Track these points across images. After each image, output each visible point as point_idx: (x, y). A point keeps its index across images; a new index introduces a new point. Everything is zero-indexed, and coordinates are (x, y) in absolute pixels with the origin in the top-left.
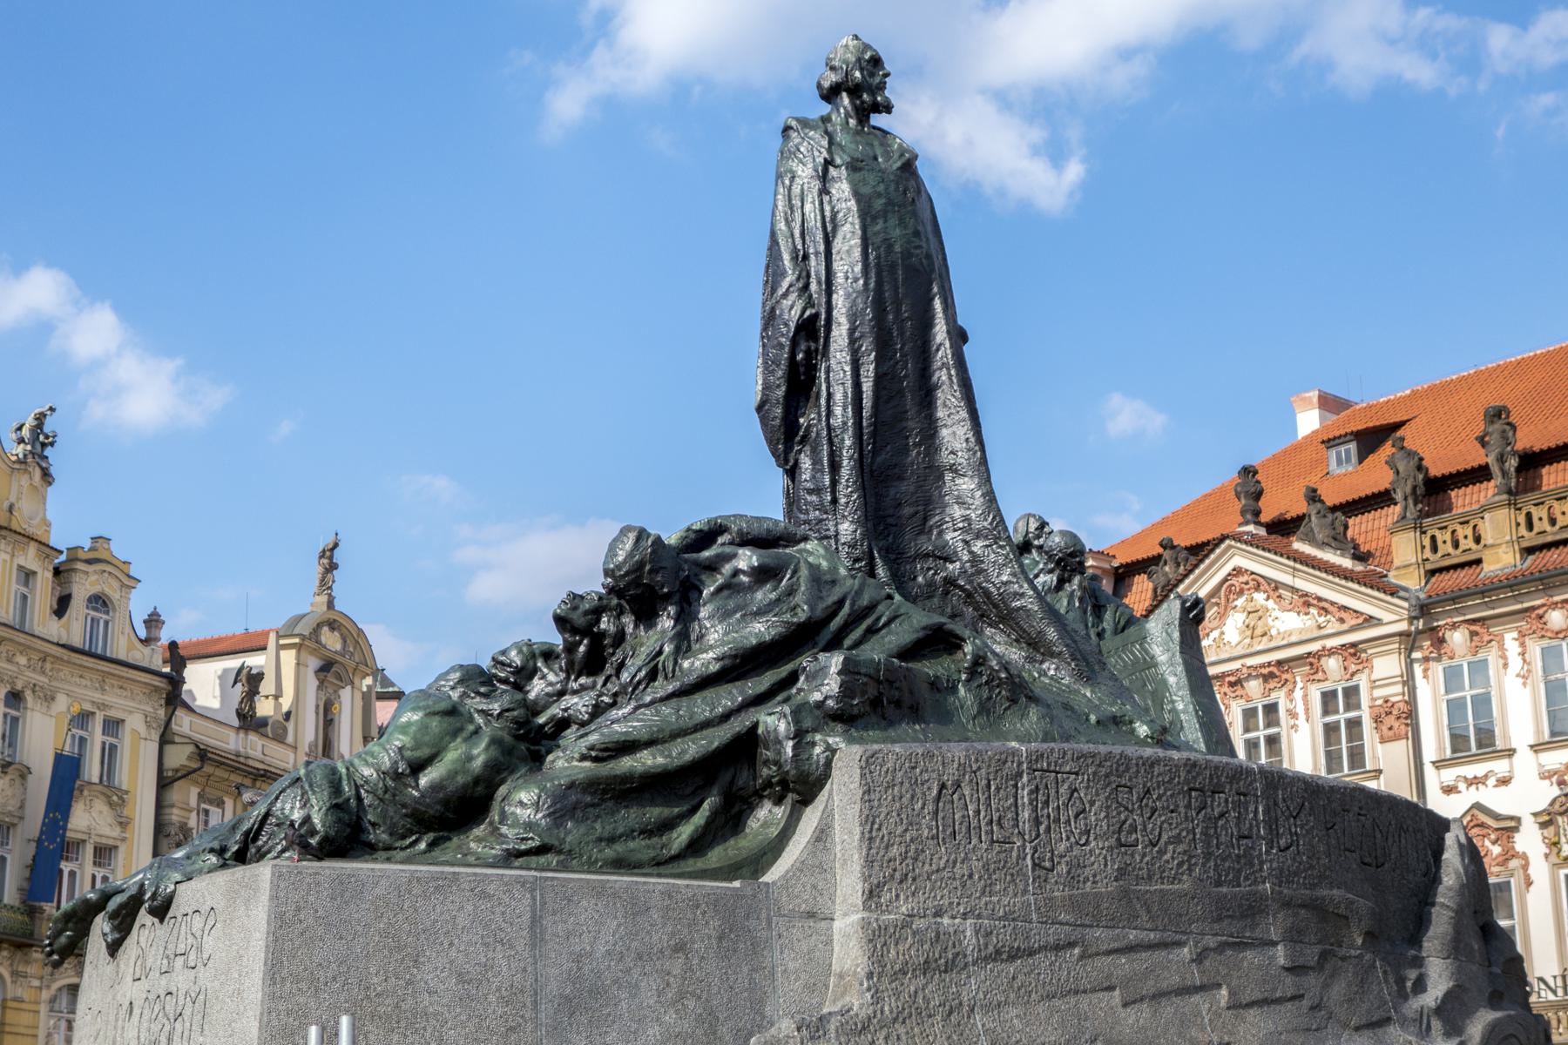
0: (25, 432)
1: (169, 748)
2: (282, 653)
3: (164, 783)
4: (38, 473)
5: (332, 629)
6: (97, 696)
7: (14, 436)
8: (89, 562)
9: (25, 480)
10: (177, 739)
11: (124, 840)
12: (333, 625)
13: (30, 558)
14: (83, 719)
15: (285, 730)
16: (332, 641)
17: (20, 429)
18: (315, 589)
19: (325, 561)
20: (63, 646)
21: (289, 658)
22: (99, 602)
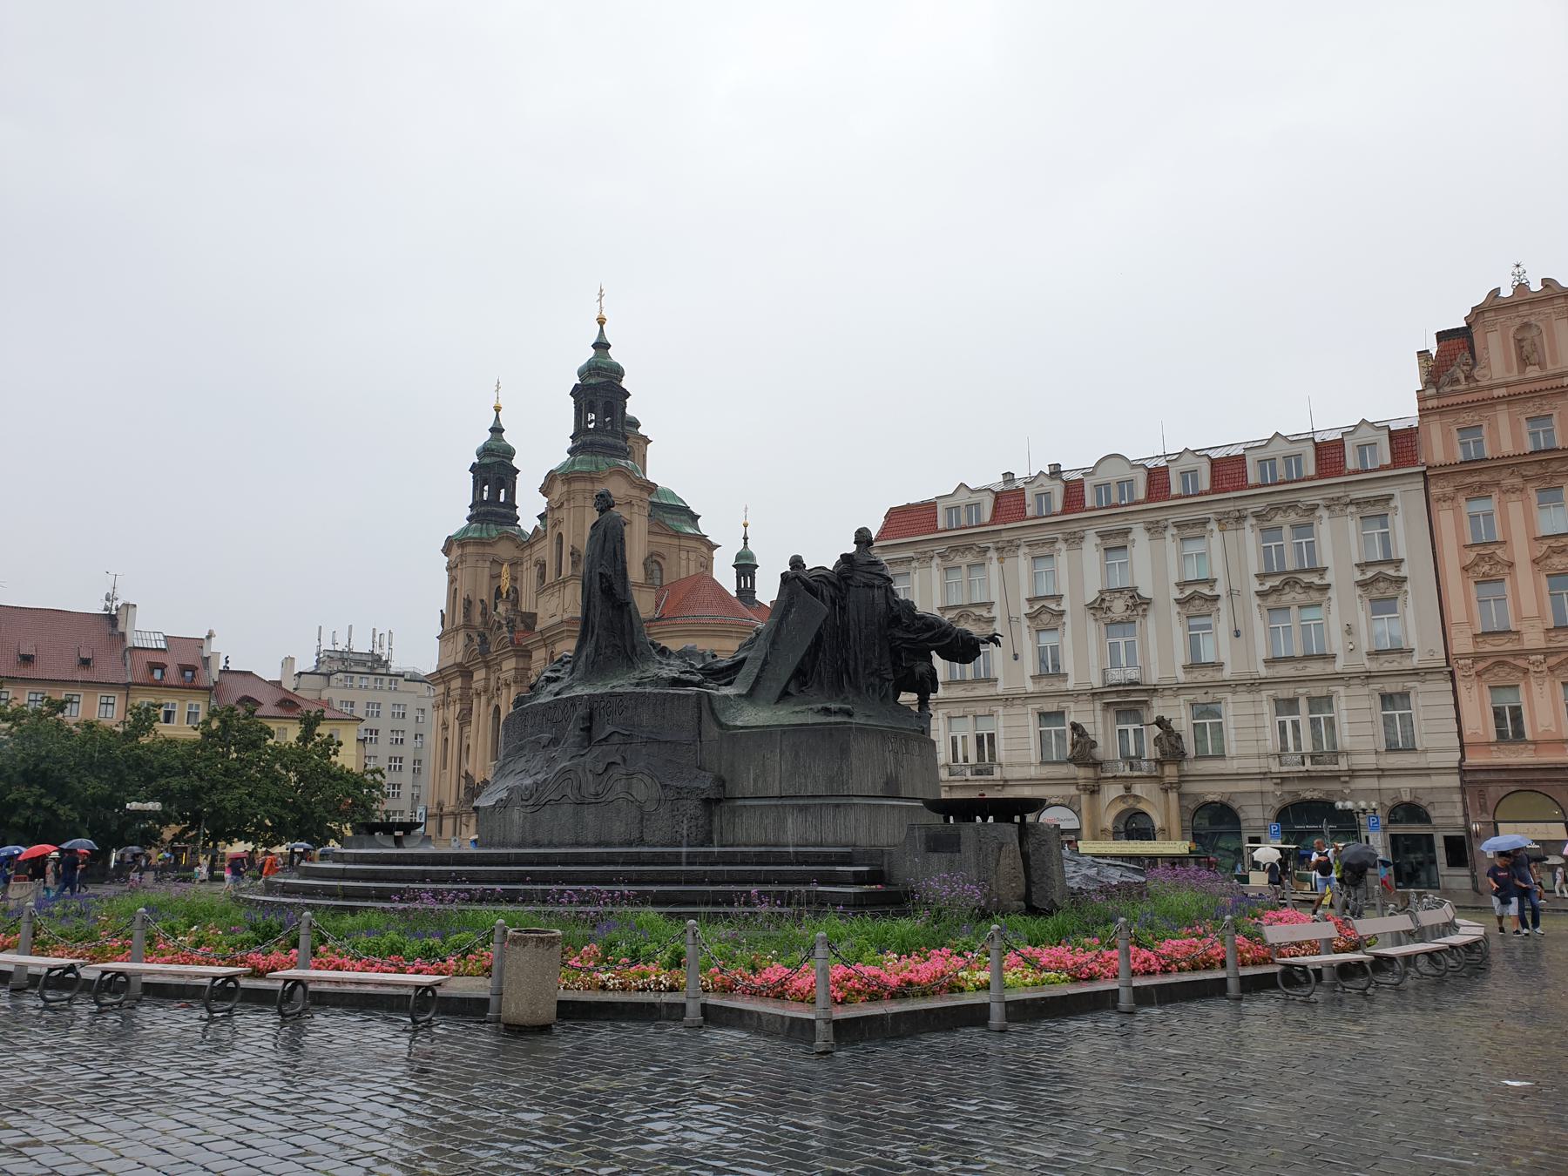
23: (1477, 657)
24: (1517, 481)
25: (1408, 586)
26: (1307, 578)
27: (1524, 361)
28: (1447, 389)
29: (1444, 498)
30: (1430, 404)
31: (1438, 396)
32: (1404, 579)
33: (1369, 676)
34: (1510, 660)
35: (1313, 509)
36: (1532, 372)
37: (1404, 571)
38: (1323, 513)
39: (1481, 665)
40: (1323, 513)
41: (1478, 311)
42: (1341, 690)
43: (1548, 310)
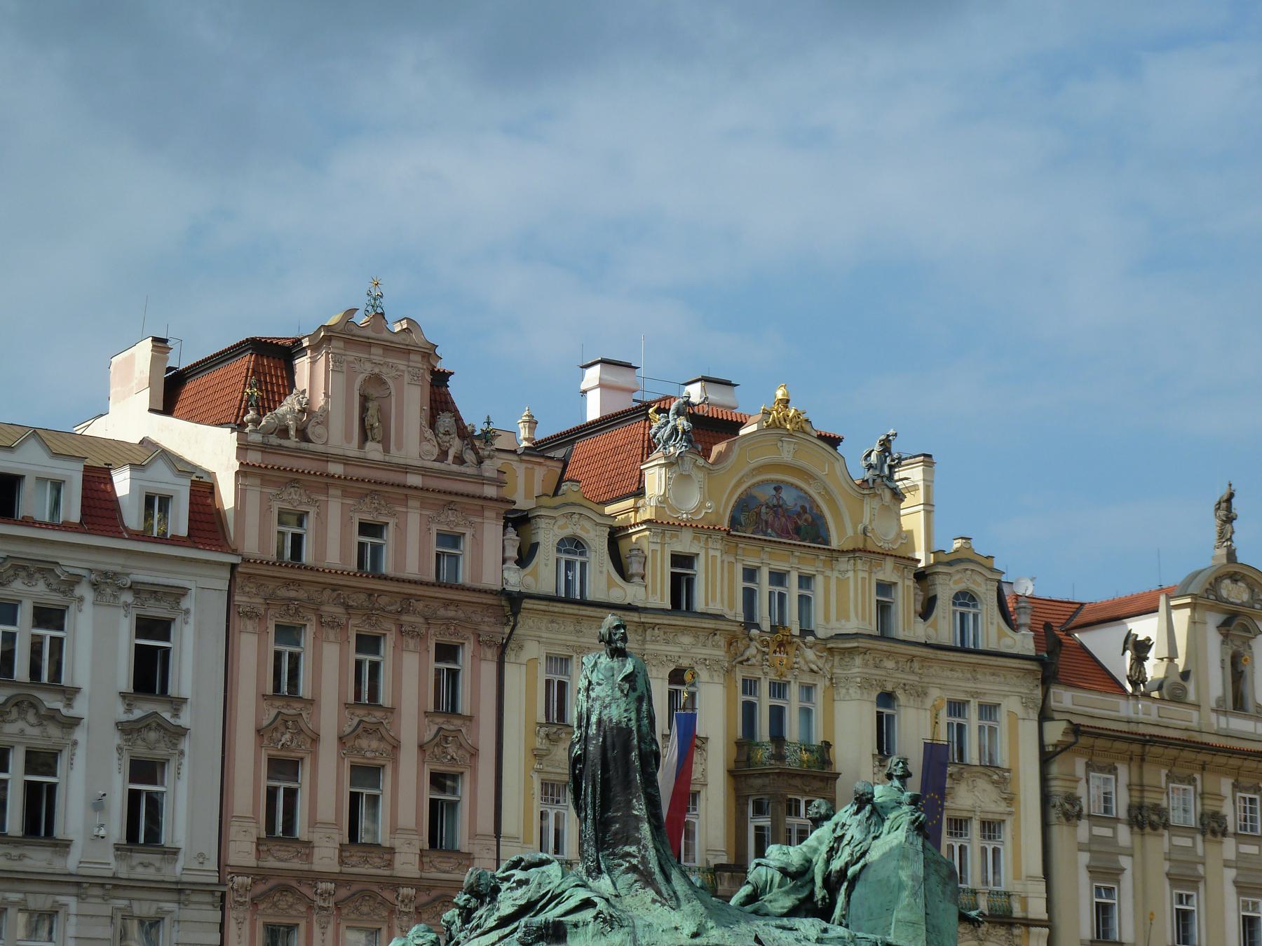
0: (873, 459)
1: (1048, 726)
2: (1176, 615)
3: (1046, 758)
4: (887, 495)
5: (1235, 581)
6: (970, 686)
7: (864, 464)
8: (950, 564)
9: (876, 503)
10: (1056, 716)
11: (1010, 814)
12: (1234, 577)
13: (888, 572)
14: (957, 708)
15: (1185, 690)
16: (1236, 593)
17: (869, 455)
18: (1215, 543)
19: (1222, 513)
20: (926, 645)
21: (1181, 618)
22: (965, 598)
23: (259, 875)
24: (339, 610)
25: (185, 745)
26: (52, 702)
27: (365, 436)
28: (274, 440)
29: (250, 615)
30: (254, 457)
31: (264, 448)
32: (181, 732)
33: (112, 886)
34: (294, 884)
35: (75, 580)
36: (373, 451)
37: (185, 719)
38: (84, 590)
39: (261, 888)
40: (84, 590)
41: (328, 337)
42: (72, 903)
43: (401, 364)
